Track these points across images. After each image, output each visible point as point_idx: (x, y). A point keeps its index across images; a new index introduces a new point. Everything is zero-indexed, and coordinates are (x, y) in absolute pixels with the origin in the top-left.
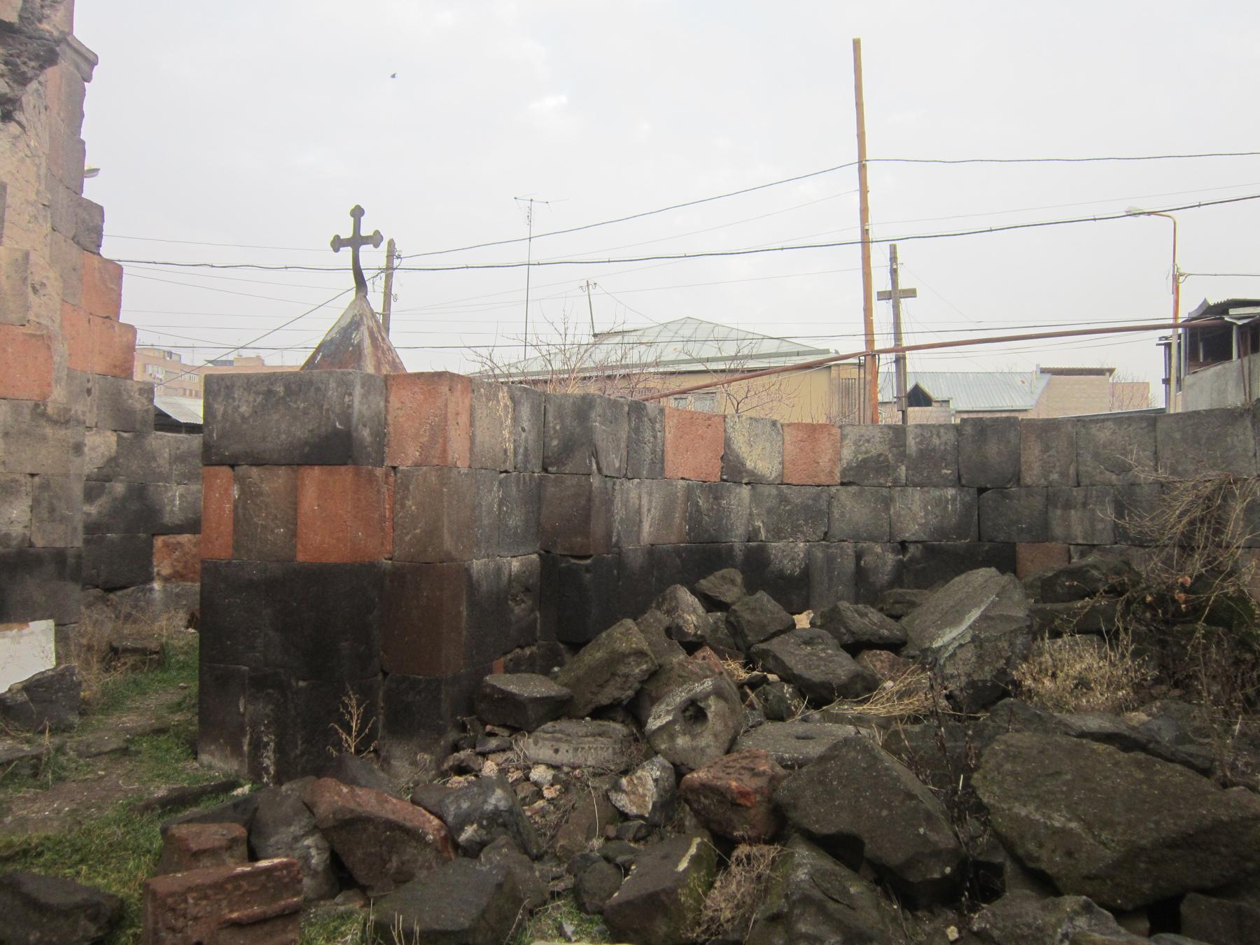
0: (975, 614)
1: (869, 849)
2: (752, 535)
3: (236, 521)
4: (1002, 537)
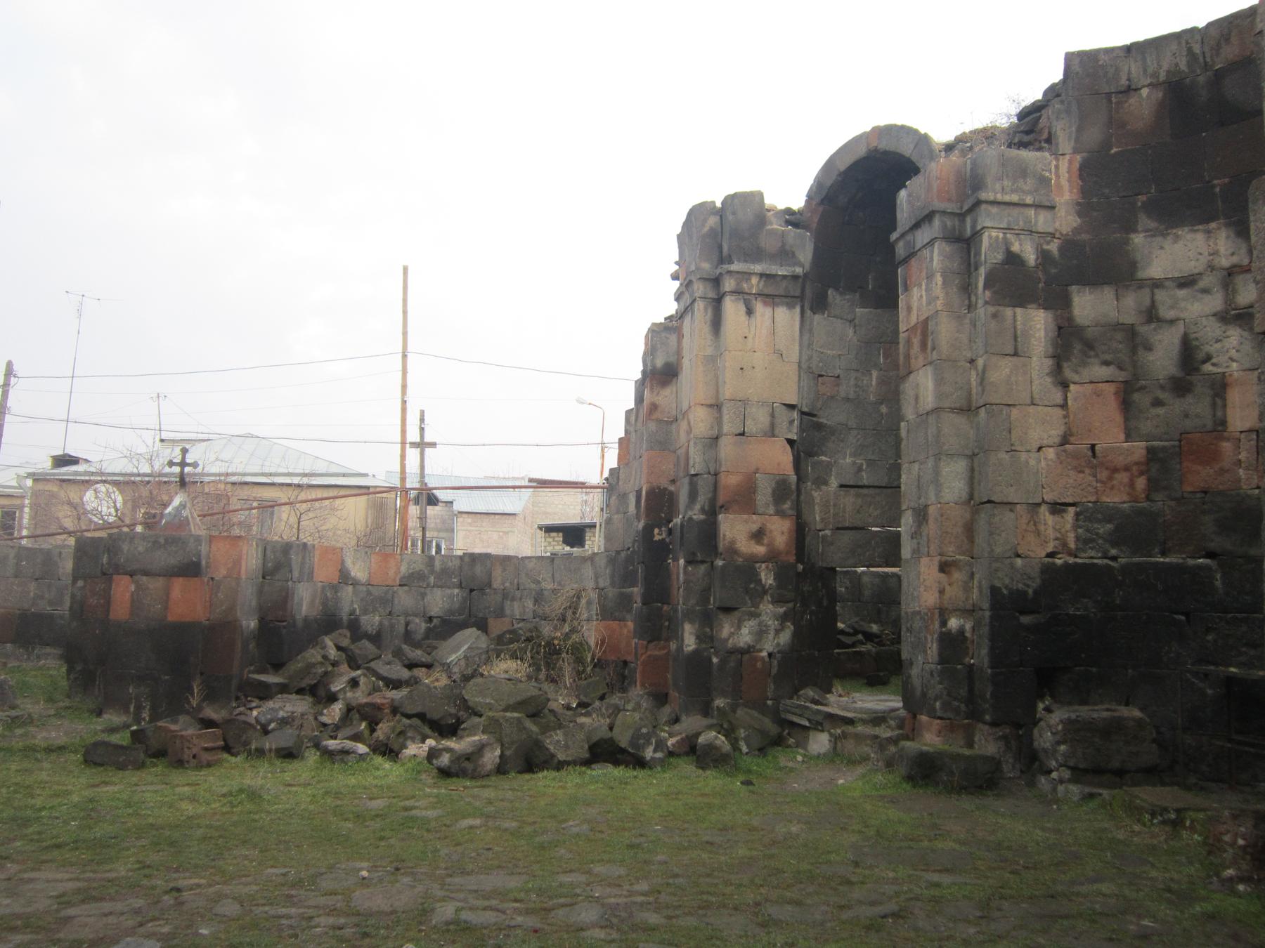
0: (466, 647)
1: (428, 716)
2: (352, 612)
3: (133, 601)
4: (481, 615)
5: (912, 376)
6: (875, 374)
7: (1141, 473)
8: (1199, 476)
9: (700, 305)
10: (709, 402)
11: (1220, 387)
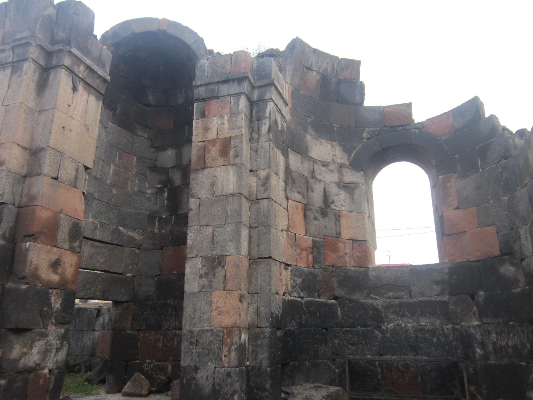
5: (206, 171)
6: (112, 167)
7: (311, 253)
8: (331, 258)
9: (29, 67)
10: (24, 145)
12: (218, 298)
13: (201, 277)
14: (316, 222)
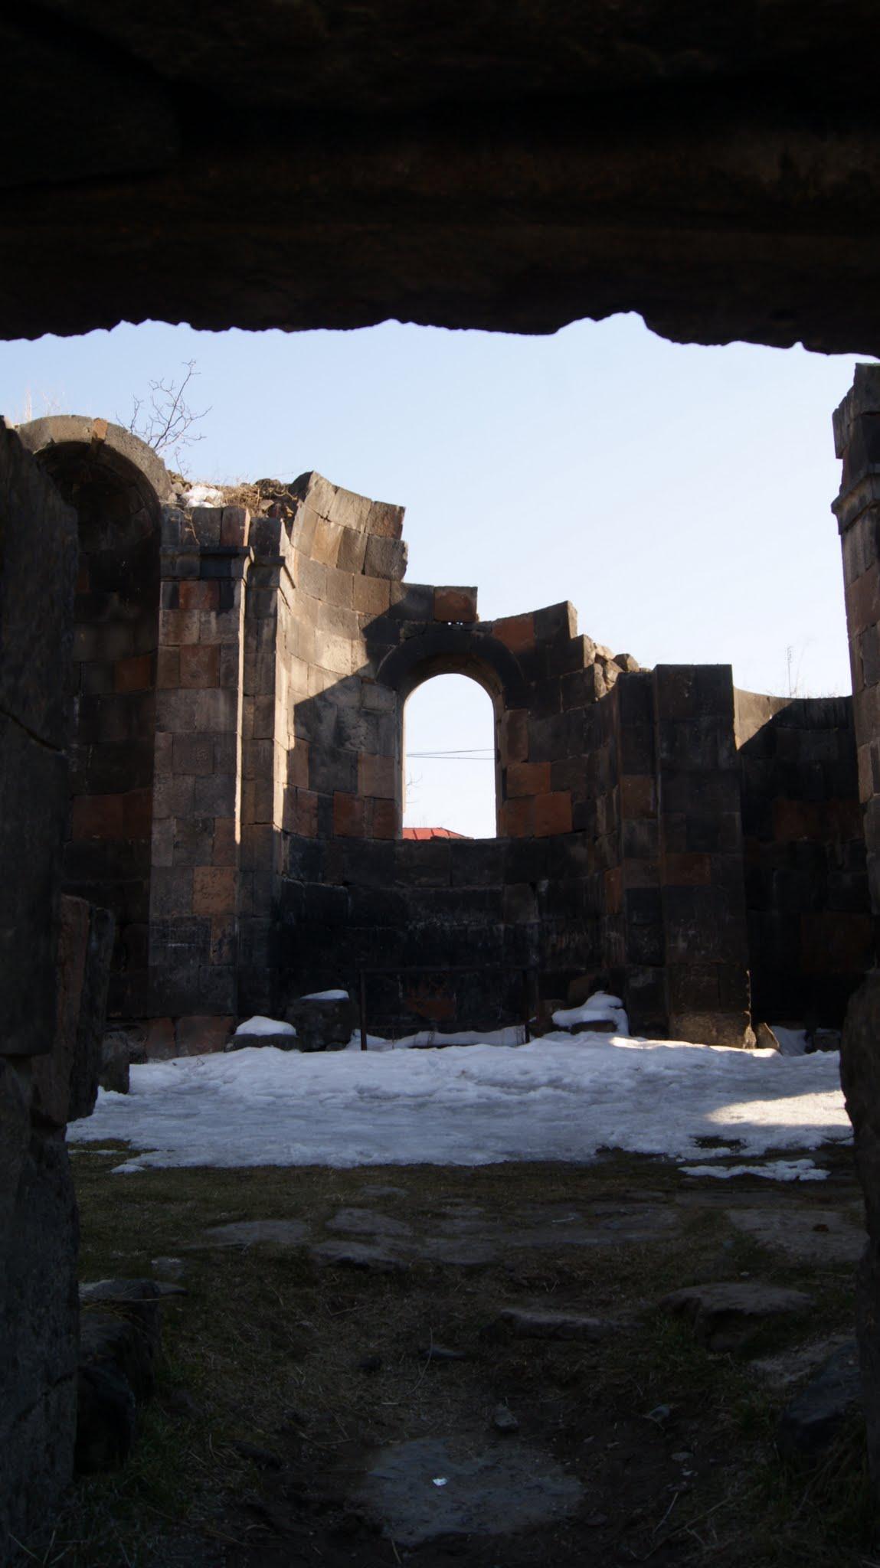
5: (182, 693)
11: (354, 761)
12: (202, 875)
13: (176, 846)
14: (323, 770)
